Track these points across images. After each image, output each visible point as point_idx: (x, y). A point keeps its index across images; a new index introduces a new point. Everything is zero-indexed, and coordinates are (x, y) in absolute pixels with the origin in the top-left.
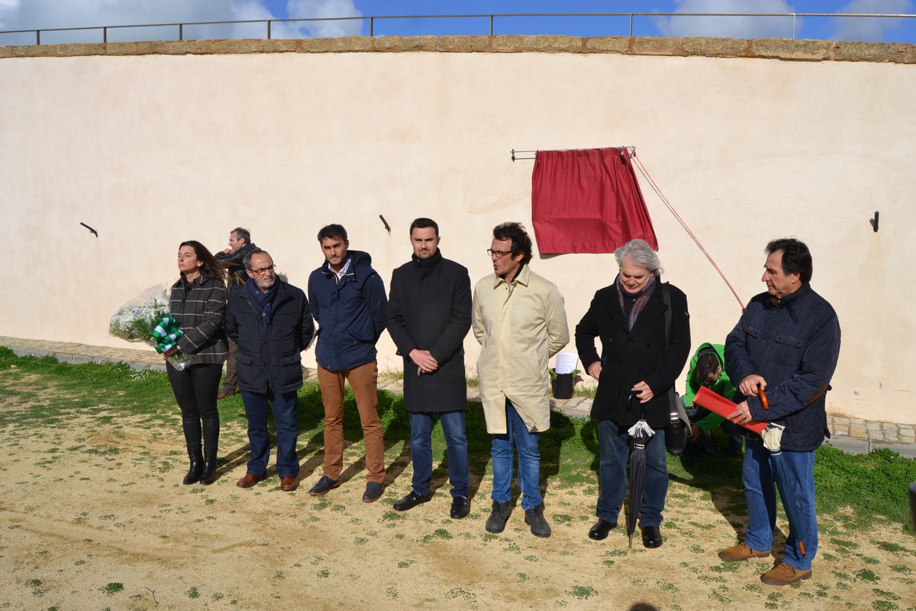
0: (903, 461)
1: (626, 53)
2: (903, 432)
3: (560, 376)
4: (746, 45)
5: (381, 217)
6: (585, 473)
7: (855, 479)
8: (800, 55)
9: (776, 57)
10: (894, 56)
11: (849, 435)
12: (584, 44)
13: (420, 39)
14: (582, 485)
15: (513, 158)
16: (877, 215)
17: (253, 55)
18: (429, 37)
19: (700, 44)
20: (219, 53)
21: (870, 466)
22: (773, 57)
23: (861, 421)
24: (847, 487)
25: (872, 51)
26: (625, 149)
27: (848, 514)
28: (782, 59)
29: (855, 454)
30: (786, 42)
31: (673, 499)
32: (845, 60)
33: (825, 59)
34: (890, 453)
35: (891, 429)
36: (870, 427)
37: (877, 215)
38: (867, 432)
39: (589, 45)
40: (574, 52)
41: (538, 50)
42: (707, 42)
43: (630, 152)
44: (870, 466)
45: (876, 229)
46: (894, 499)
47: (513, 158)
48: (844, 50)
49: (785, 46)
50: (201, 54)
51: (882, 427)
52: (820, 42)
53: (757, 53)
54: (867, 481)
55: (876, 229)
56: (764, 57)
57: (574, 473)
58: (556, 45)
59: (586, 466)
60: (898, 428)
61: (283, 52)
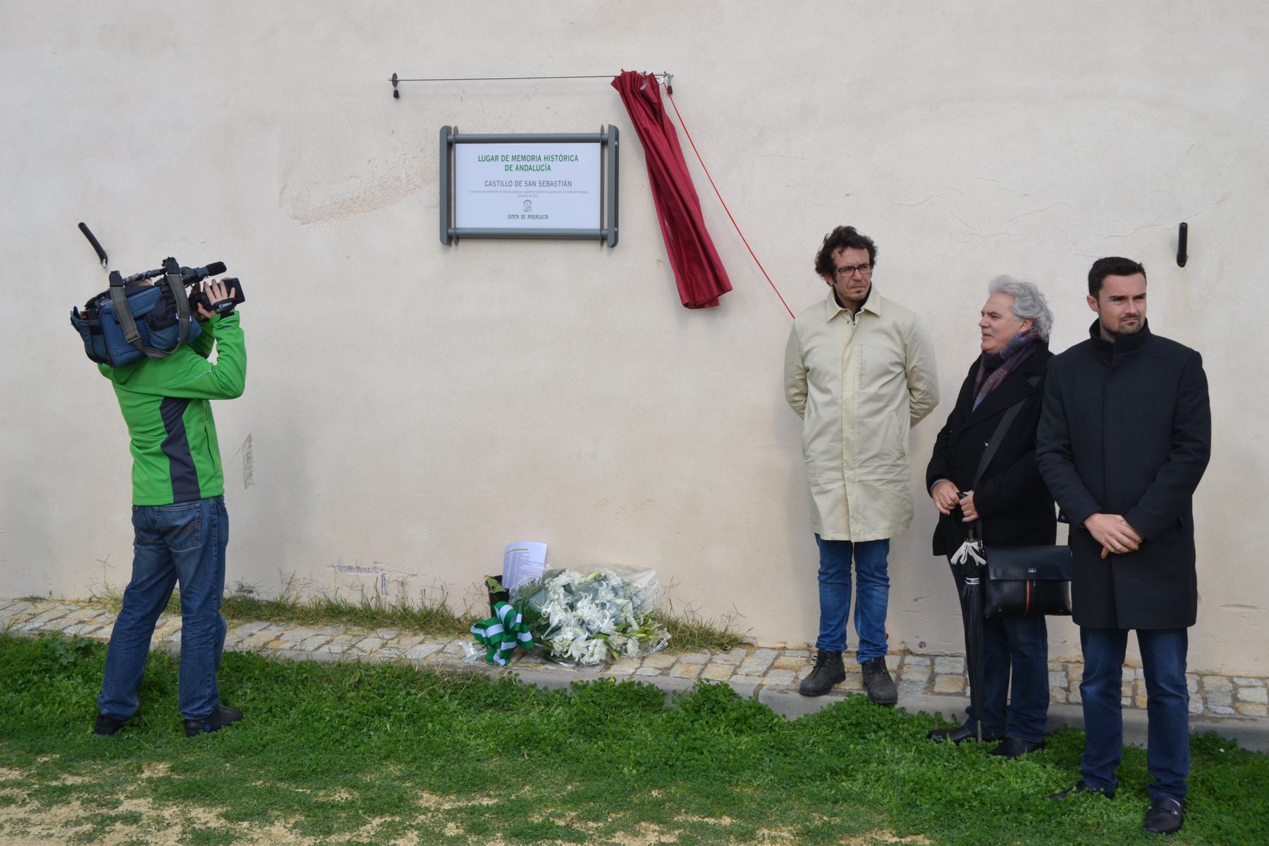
2: (1243, 694)
6: (561, 816)
35: (1219, 688)
45: (1182, 259)
57: (537, 819)
59: (564, 802)
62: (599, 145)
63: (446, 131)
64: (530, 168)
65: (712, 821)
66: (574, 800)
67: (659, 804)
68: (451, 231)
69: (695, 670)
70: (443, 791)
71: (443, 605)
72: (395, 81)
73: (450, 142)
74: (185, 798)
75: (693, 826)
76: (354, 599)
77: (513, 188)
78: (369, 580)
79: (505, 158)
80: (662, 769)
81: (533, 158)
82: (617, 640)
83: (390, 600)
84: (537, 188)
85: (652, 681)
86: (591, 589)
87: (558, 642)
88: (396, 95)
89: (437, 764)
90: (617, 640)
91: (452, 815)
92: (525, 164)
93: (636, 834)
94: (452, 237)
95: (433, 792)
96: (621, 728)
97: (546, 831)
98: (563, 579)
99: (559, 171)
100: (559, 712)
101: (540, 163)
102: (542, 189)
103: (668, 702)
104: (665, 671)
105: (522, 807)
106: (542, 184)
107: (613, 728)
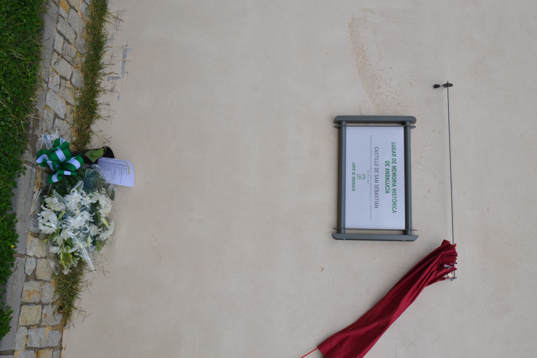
62: (403, 228)
63: (413, 120)
64: (387, 179)
68: (344, 123)
71: (99, 117)
72: (448, 85)
73: (405, 123)
76: (105, 59)
77: (374, 167)
78: (117, 69)
79: (394, 161)
81: (394, 181)
82: (59, 239)
83: (104, 83)
84: (374, 184)
85: (20, 268)
86: (96, 220)
87: (54, 201)
88: (436, 86)
90: (60, 242)
92: (390, 175)
94: (340, 124)
98: (104, 201)
99: (386, 199)
101: (391, 185)
102: (373, 187)
106: (376, 187)
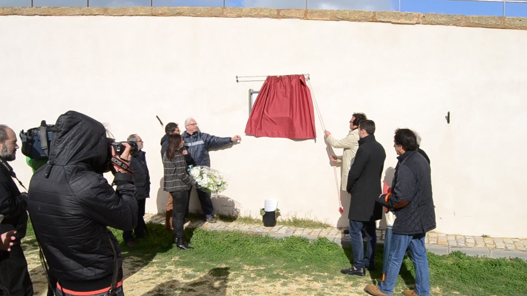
0: (469, 258)
1: (303, 18)
2: (467, 240)
3: (267, 213)
4: (372, 15)
5: (157, 117)
6: (282, 272)
7: (441, 270)
8: (403, 21)
9: (390, 22)
10: (455, 22)
11: (437, 244)
12: (278, 13)
13: (180, 9)
14: (280, 280)
15: (237, 81)
16: (449, 114)
17: (77, 17)
18: (186, 7)
19: (346, 14)
20: (56, 15)
21: (450, 262)
22: (388, 22)
23: (444, 235)
24: (437, 274)
25: (443, 19)
26: (303, 76)
27: (437, 292)
28: (393, 23)
29: (441, 255)
30: (395, 13)
31: (334, 287)
32: (428, 24)
33: (417, 23)
34: (461, 254)
35: (461, 239)
36: (449, 238)
37: (449, 114)
38: (448, 241)
39: (281, 14)
40: (273, 18)
41: (251, 16)
42: (350, 13)
43: (306, 77)
44: (450, 262)
45: (448, 122)
46: (464, 281)
47: (237, 81)
48: (427, 18)
49: (395, 16)
50: (44, 15)
51: (456, 238)
52: (414, 13)
53: (379, 20)
54: (448, 271)
55: (448, 122)
56: (383, 22)
57: (275, 273)
58: (262, 13)
60: (465, 239)
61: (96, 15)
65: (322, 274)
66: (285, 268)
67: (307, 269)
69: (317, 233)
70: (251, 265)
74: (183, 265)
75: (317, 275)
80: (308, 260)
89: (248, 258)
91: (252, 271)
93: (302, 277)
95: (248, 265)
96: (297, 248)
97: (278, 276)
100: (281, 245)
103: (310, 242)
104: (309, 234)
105: (271, 270)
107: (295, 249)
